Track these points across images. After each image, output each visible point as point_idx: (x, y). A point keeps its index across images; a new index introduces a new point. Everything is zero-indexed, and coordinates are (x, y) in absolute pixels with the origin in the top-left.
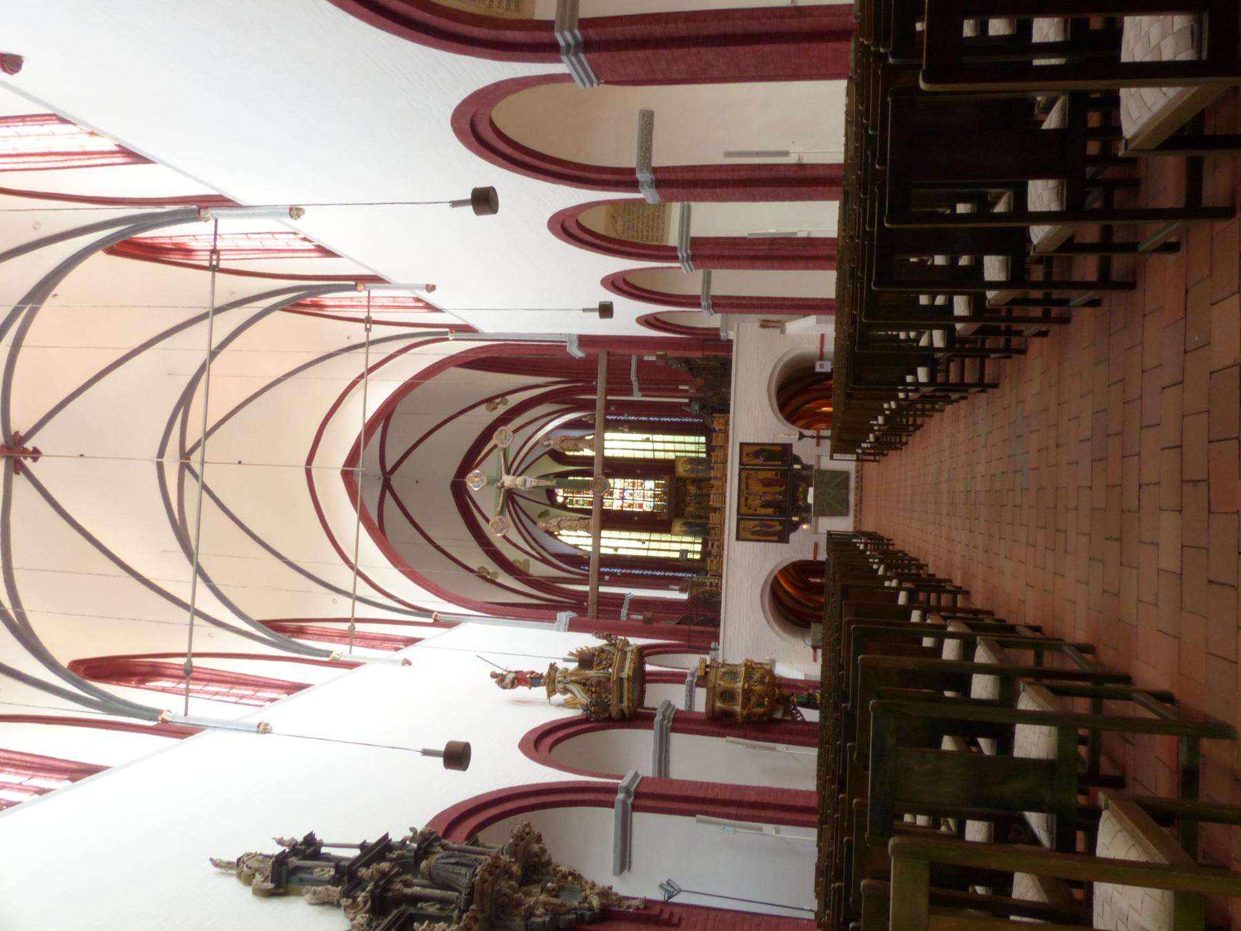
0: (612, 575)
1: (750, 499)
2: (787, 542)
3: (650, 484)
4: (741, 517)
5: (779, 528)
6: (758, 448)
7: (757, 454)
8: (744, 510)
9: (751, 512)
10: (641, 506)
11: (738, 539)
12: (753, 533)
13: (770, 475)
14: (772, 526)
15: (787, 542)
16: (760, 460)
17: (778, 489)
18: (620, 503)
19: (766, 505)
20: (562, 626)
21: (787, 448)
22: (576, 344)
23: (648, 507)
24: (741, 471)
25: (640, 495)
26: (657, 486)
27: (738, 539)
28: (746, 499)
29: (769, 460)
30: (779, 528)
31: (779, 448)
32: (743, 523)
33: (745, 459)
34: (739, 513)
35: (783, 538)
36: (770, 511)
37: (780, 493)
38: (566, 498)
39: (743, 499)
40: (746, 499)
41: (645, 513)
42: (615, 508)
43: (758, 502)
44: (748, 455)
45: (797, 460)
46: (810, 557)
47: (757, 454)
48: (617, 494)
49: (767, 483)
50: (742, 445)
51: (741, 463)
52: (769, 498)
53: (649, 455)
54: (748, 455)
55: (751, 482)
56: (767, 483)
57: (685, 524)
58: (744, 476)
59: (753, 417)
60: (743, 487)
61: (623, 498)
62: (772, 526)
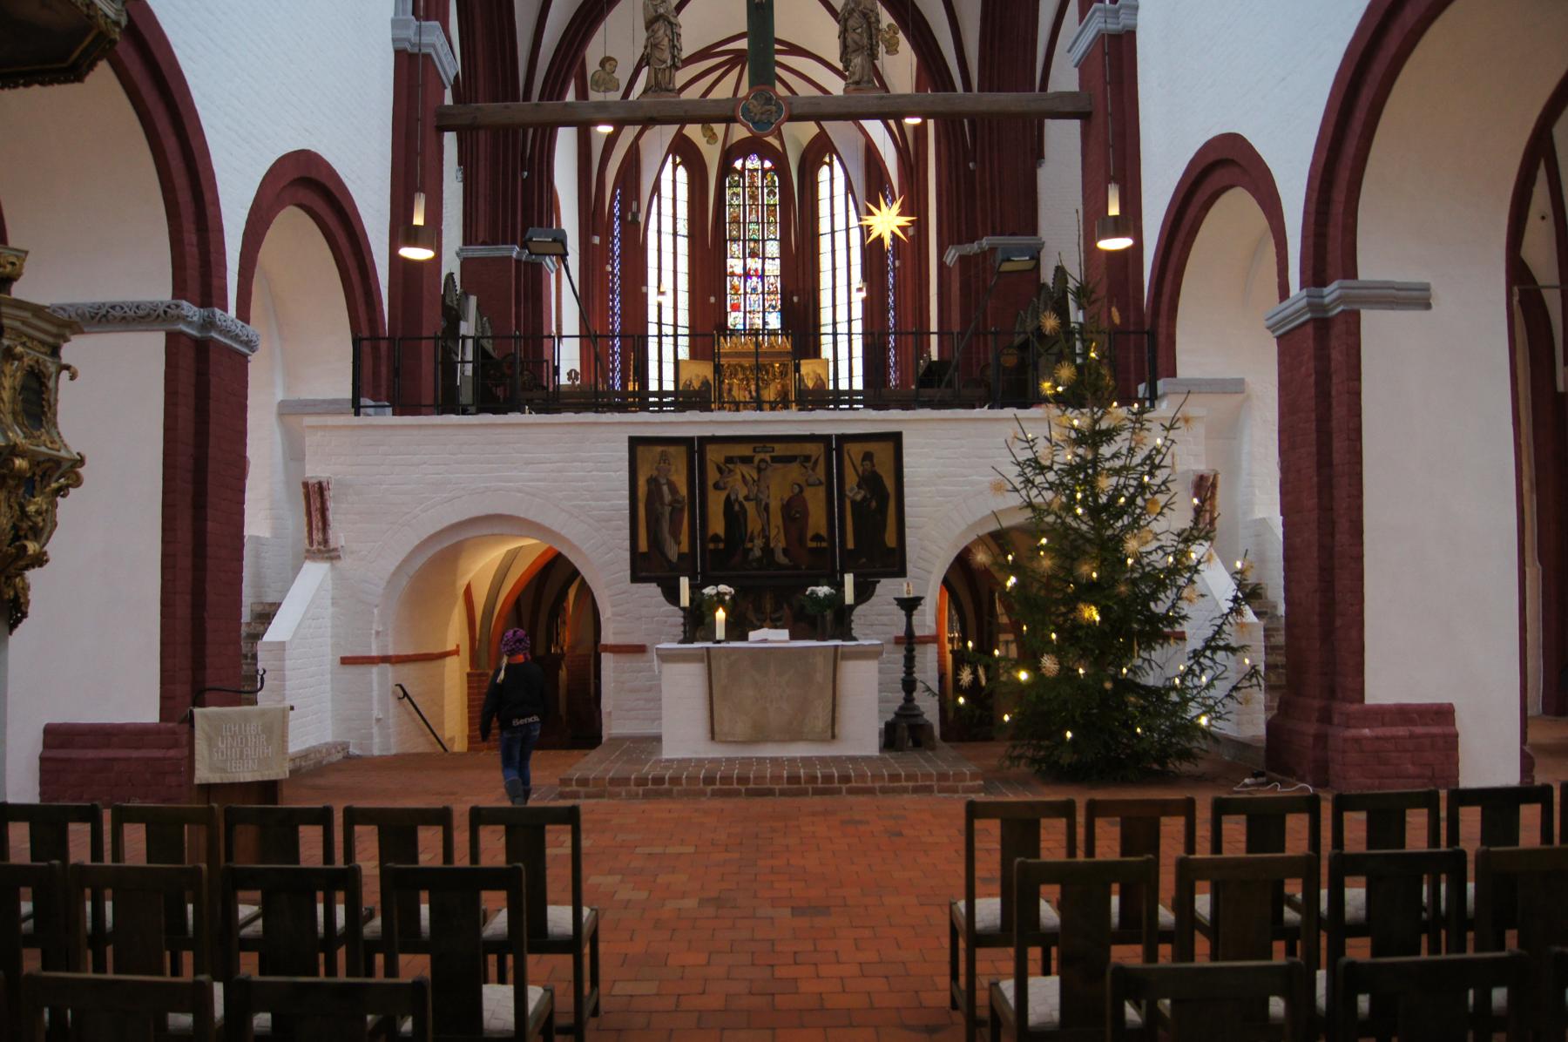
0: (605, 253)
1: (750, 472)
2: (635, 578)
3: (774, 321)
4: (696, 448)
5: (672, 553)
6: (889, 484)
7: (871, 481)
8: (714, 455)
9: (713, 476)
10: (736, 308)
11: (635, 442)
12: (653, 482)
13: (817, 520)
14: (676, 534)
15: (635, 578)
17: (779, 543)
18: (739, 270)
19: (734, 515)
20: (411, 33)
21: (896, 564)
22: (1112, 27)
23: (735, 320)
24: (826, 439)
25: (754, 309)
26: (773, 333)
27: (635, 442)
28: (746, 460)
29: (863, 517)
30: (672, 553)
31: (890, 540)
32: (678, 456)
33: (855, 450)
34: (704, 440)
35: (648, 565)
36: (717, 526)
37: (768, 550)
38: (741, 173)
39: (745, 450)
40: (746, 460)
41: (726, 314)
42: (730, 262)
43: (742, 492)
44: (868, 456)
45: (864, 592)
46: (608, 636)
47: (871, 481)
48: (755, 264)
49: (794, 512)
50: (895, 439)
51: (843, 439)
52: (754, 524)
53: (826, 316)
54: (868, 456)
55: (795, 472)
56: (794, 512)
57: (706, 383)
58: (814, 450)
59: (965, 473)
60: (780, 449)
61: (747, 275)
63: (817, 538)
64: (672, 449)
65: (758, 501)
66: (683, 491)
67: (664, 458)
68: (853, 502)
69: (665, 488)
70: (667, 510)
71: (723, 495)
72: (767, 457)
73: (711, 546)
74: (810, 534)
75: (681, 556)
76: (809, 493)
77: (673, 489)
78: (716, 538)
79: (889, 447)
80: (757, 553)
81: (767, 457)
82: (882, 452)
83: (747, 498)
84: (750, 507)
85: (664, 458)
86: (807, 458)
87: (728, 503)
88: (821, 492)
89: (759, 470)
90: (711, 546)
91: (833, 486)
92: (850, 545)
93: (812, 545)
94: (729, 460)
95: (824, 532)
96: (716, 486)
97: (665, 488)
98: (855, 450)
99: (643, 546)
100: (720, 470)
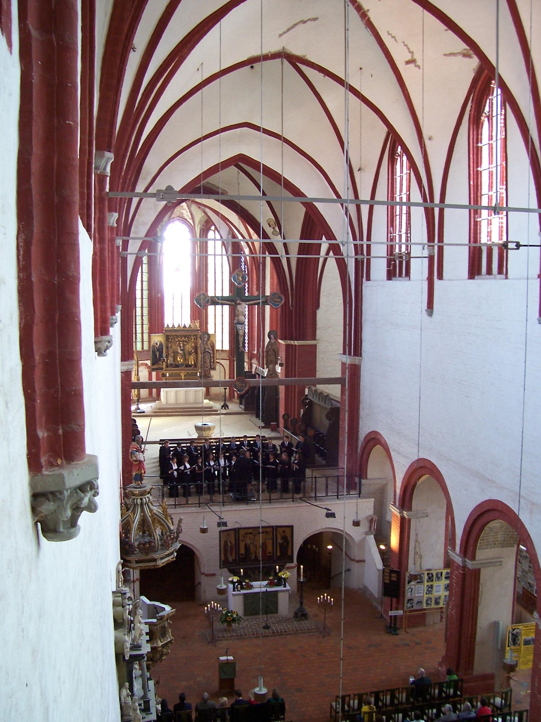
5: (230, 559)
6: (289, 539)
7: (285, 538)
8: (242, 532)
12: (226, 542)
13: (270, 548)
16: (280, 541)
19: (247, 548)
24: (272, 527)
28: (251, 533)
30: (230, 559)
32: (233, 532)
33: (280, 530)
35: (224, 563)
36: (242, 551)
37: (256, 557)
39: (250, 531)
40: (251, 533)
43: (248, 541)
44: (284, 531)
47: (285, 538)
52: (252, 549)
54: (284, 531)
58: (270, 530)
62: (231, 555)
63: (269, 553)
64: (231, 532)
65: (254, 544)
66: (233, 542)
67: (229, 535)
68: (280, 544)
69: (229, 543)
70: (229, 549)
71: (244, 543)
72: (256, 532)
73: (241, 557)
74: (267, 552)
75: (233, 560)
76: (267, 541)
77: (231, 543)
78: (242, 554)
79: (290, 529)
80: (253, 557)
81: (256, 532)
82: (288, 531)
83: (251, 543)
84: (252, 546)
85: (229, 535)
86: (267, 532)
87: (246, 545)
88: (271, 541)
89: (254, 536)
90: (241, 557)
91: (274, 539)
92: (278, 554)
93: (268, 555)
94: (246, 534)
95: (271, 551)
96: (242, 541)
97: (229, 543)
98: (280, 530)
99: (223, 558)
100: (244, 537)
